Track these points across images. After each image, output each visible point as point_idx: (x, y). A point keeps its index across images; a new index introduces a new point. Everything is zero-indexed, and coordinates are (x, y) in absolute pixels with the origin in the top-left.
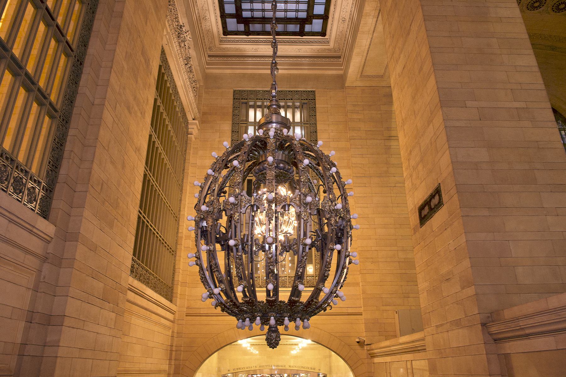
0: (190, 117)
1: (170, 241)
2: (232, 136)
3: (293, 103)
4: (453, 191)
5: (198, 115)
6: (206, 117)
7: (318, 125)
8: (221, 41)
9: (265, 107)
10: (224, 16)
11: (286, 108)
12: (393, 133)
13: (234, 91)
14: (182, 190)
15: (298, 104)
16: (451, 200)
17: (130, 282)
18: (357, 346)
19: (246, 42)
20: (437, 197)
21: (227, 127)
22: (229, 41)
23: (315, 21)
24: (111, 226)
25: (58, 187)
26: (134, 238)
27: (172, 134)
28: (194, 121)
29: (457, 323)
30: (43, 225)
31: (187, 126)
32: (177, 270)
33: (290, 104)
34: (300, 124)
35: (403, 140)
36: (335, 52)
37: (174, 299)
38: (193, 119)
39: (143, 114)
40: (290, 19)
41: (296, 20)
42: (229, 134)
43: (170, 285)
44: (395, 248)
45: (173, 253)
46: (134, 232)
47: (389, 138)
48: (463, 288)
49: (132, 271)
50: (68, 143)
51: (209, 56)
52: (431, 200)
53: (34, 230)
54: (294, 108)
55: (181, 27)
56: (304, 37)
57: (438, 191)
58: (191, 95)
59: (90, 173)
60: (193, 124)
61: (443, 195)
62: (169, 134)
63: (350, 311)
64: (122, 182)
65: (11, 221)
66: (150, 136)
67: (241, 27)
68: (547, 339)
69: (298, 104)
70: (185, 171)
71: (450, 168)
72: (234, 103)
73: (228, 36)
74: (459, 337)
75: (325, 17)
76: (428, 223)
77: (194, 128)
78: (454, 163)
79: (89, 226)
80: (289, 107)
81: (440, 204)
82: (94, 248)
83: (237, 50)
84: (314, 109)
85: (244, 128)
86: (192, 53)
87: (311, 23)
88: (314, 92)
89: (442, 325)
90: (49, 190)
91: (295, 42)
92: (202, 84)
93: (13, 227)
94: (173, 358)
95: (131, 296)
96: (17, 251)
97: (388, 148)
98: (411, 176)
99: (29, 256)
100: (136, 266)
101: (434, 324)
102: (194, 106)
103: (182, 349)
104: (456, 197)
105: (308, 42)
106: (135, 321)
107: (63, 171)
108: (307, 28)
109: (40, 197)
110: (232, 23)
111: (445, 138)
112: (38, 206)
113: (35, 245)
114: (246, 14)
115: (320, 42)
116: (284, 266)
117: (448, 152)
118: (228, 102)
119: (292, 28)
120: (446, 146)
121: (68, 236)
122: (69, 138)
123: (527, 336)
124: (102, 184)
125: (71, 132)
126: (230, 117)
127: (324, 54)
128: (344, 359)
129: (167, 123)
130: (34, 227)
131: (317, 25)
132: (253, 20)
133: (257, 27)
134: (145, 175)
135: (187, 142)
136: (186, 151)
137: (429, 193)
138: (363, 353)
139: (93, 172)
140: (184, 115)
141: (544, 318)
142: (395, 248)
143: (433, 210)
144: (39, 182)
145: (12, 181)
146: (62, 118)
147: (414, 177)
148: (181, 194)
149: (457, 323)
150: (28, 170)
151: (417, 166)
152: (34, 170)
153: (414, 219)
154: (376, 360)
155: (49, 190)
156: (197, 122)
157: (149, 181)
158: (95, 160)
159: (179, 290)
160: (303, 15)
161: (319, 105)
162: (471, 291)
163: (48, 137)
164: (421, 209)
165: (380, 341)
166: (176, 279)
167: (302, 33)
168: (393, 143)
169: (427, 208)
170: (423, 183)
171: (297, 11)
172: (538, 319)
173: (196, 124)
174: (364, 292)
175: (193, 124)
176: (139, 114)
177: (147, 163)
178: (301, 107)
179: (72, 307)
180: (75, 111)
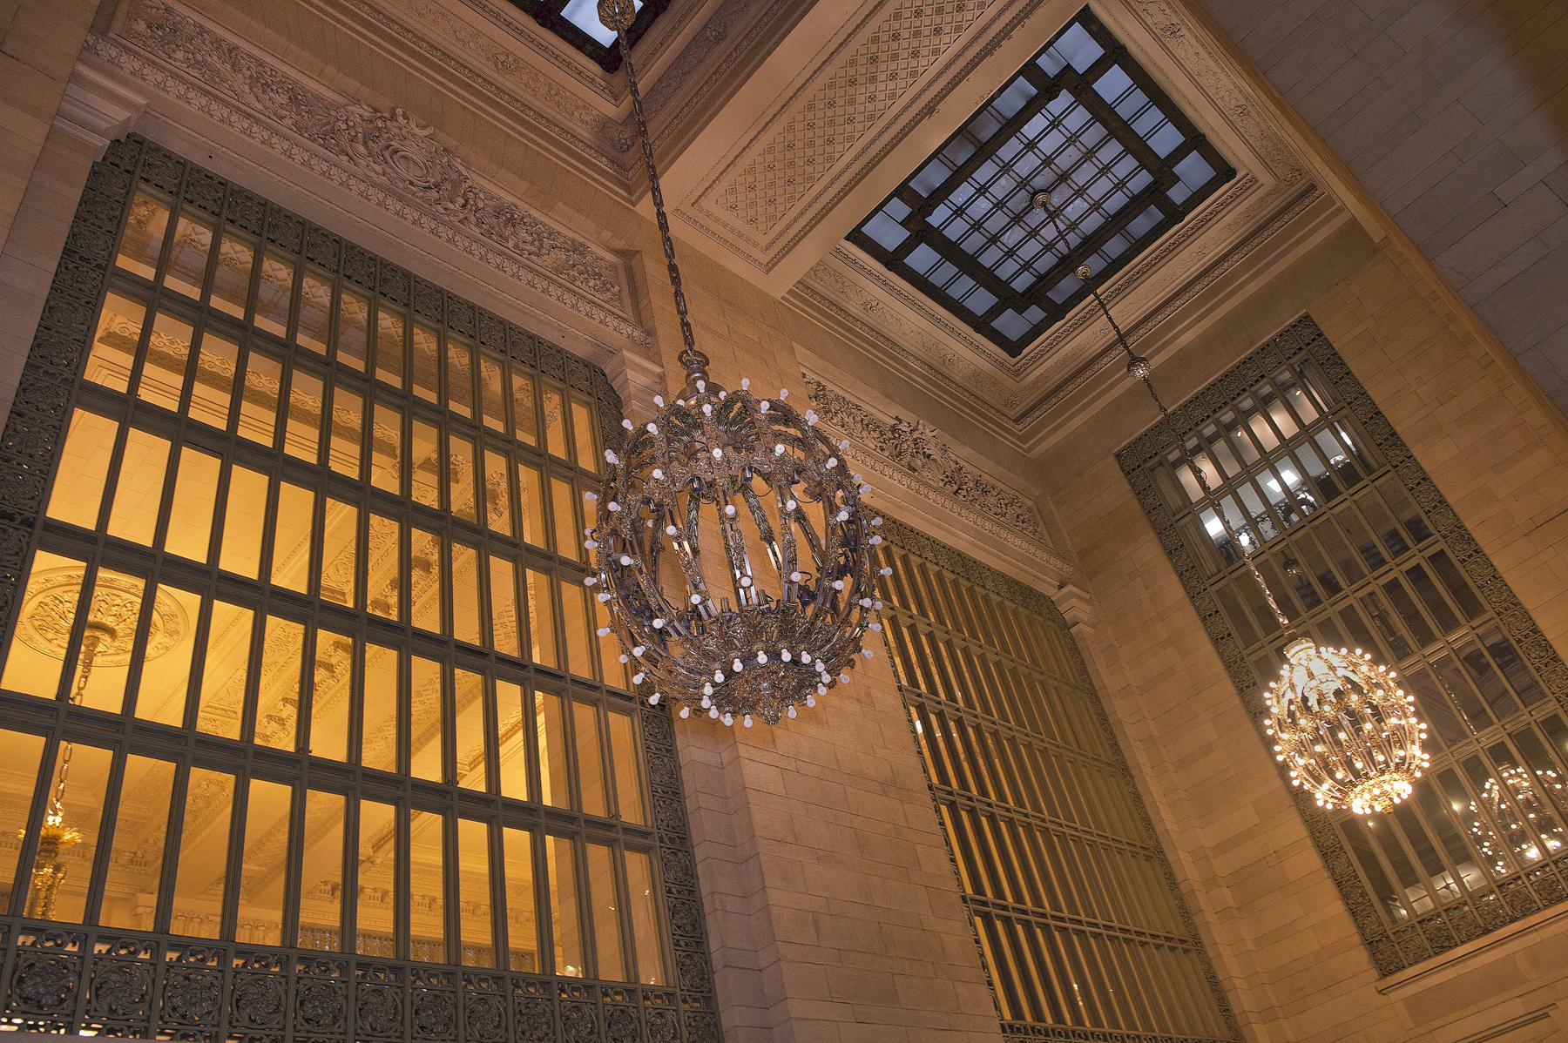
6: (1089, 564)
7: (1371, 393)
8: (1018, 373)
10: (982, 324)
13: (1118, 456)
19: (1068, 332)
22: (1034, 360)
23: (1178, 169)
33: (1267, 389)
36: (1292, 185)
38: (1060, 587)
40: (1119, 212)
41: (1137, 204)
51: (1016, 421)
55: (894, 429)
56: (1187, 218)
58: (1014, 542)
67: (1035, 313)
70: (1110, 719)
73: (1025, 351)
75: (1195, 140)
77: (1076, 607)
83: (1064, 362)
86: (961, 452)
87: (1176, 179)
88: (1307, 317)
91: (1176, 245)
92: (1037, 493)
102: (1041, 557)
105: (1205, 222)
108: (1177, 194)
110: (1011, 323)
114: (1022, 283)
115: (1234, 197)
118: (1116, 491)
119: (1140, 225)
124: (816, 922)
127: (1272, 207)
131: (1193, 170)
132: (1046, 280)
133: (1068, 285)
146: (666, 839)
156: (1070, 587)
158: (768, 884)
160: (1143, 179)
161: (1341, 337)
167: (1174, 214)
171: (1120, 185)
180: (690, 805)
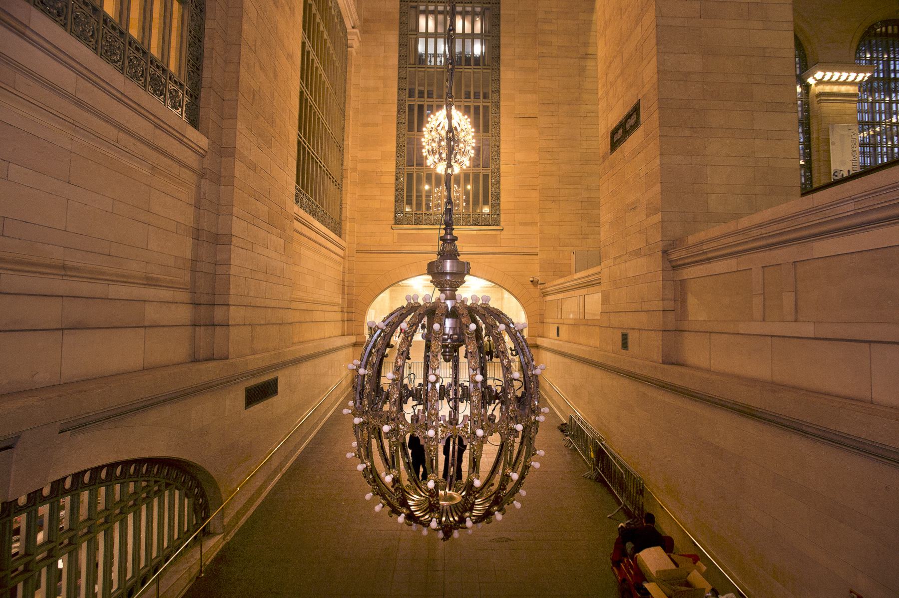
0: (348, 25)
1: (334, 171)
2: (400, 51)
3: (473, 8)
4: (655, 107)
5: (358, 23)
6: (367, 25)
9: (441, 13)
11: (464, 15)
12: (591, 50)
14: (344, 116)
15: (478, 9)
16: (650, 119)
17: (295, 211)
18: (531, 285)
20: (634, 117)
21: (393, 38)
24: (270, 146)
25: (203, 93)
26: (295, 163)
27: (328, 44)
28: (354, 30)
29: (637, 253)
30: (192, 133)
31: (346, 36)
32: (344, 206)
34: (482, 37)
35: (602, 48)
37: (343, 235)
39: (292, 9)
42: (396, 47)
43: (338, 220)
44: (579, 187)
45: (339, 186)
46: (295, 155)
47: (586, 56)
48: (648, 216)
49: (297, 201)
50: (206, 38)
52: (626, 121)
53: (185, 140)
54: (474, 14)
57: (636, 110)
59: (238, 78)
60: (352, 33)
61: (641, 114)
62: (325, 45)
63: (525, 250)
64: (276, 94)
65: (157, 126)
66: (303, 43)
68: (728, 261)
69: (478, 9)
71: (655, 80)
72: (401, 7)
74: (635, 267)
76: (619, 149)
77: (354, 39)
78: (661, 72)
79: (245, 142)
80: (467, 13)
81: (637, 123)
82: (253, 167)
84: (498, 16)
85: (413, 42)
89: (620, 256)
90: (195, 96)
93: (158, 132)
94: (346, 292)
95: (298, 225)
96: (169, 162)
97: (582, 69)
98: (607, 94)
99: (183, 169)
100: (300, 196)
101: (612, 256)
103: (354, 284)
104: (656, 115)
106: (304, 252)
107: (206, 74)
109: (185, 103)
111: (654, 41)
112: (184, 115)
113: (188, 157)
116: (458, 205)
117: (655, 59)
120: (655, 51)
121: (224, 150)
122: (207, 32)
123: (708, 260)
125: (208, 24)
126: (397, 26)
128: (516, 297)
129: (322, 28)
130: (184, 136)
134: (301, 93)
135: (346, 57)
136: (346, 68)
137: (626, 113)
138: (536, 292)
139: (241, 77)
140: (342, 21)
141: (730, 240)
142: (579, 187)
143: (627, 133)
144: (181, 84)
145: (149, 78)
147: (611, 94)
148: (344, 120)
149: (637, 253)
150: (165, 68)
151: (616, 80)
152: (173, 67)
153: (605, 144)
154: (549, 298)
155: (195, 96)
156: (357, 31)
157: (307, 100)
159: (347, 226)
162: (657, 218)
163: (182, 28)
164: (614, 133)
165: (554, 280)
166: (343, 214)
168: (590, 63)
169: (620, 132)
170: (621, 101)
172: (725, 241)
173: (356, 34)
174: (541, 232)
175: (352, 33)
176: (287, 9)
177: (302, 78)
178: (482, 15)
179: (238, 227)
